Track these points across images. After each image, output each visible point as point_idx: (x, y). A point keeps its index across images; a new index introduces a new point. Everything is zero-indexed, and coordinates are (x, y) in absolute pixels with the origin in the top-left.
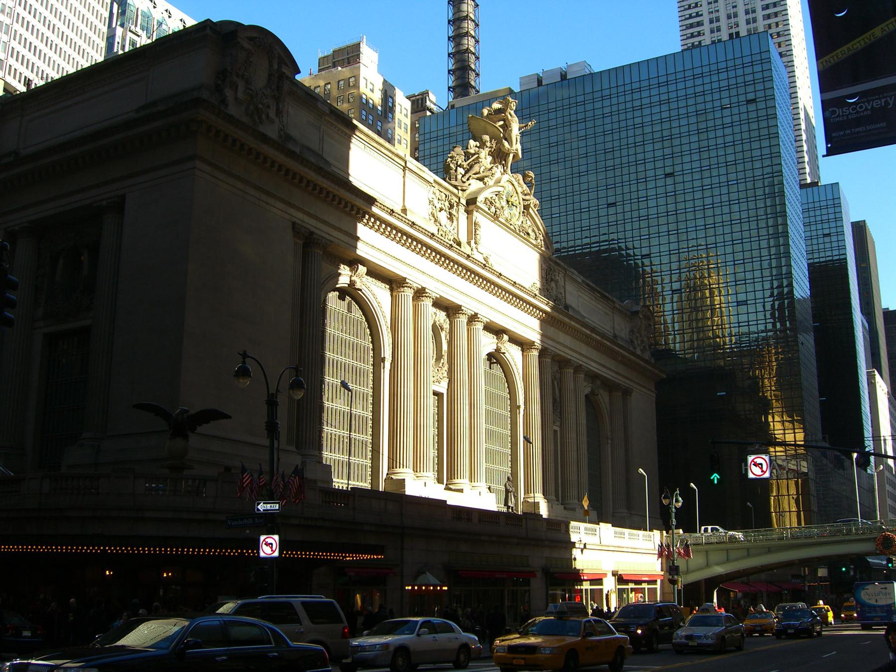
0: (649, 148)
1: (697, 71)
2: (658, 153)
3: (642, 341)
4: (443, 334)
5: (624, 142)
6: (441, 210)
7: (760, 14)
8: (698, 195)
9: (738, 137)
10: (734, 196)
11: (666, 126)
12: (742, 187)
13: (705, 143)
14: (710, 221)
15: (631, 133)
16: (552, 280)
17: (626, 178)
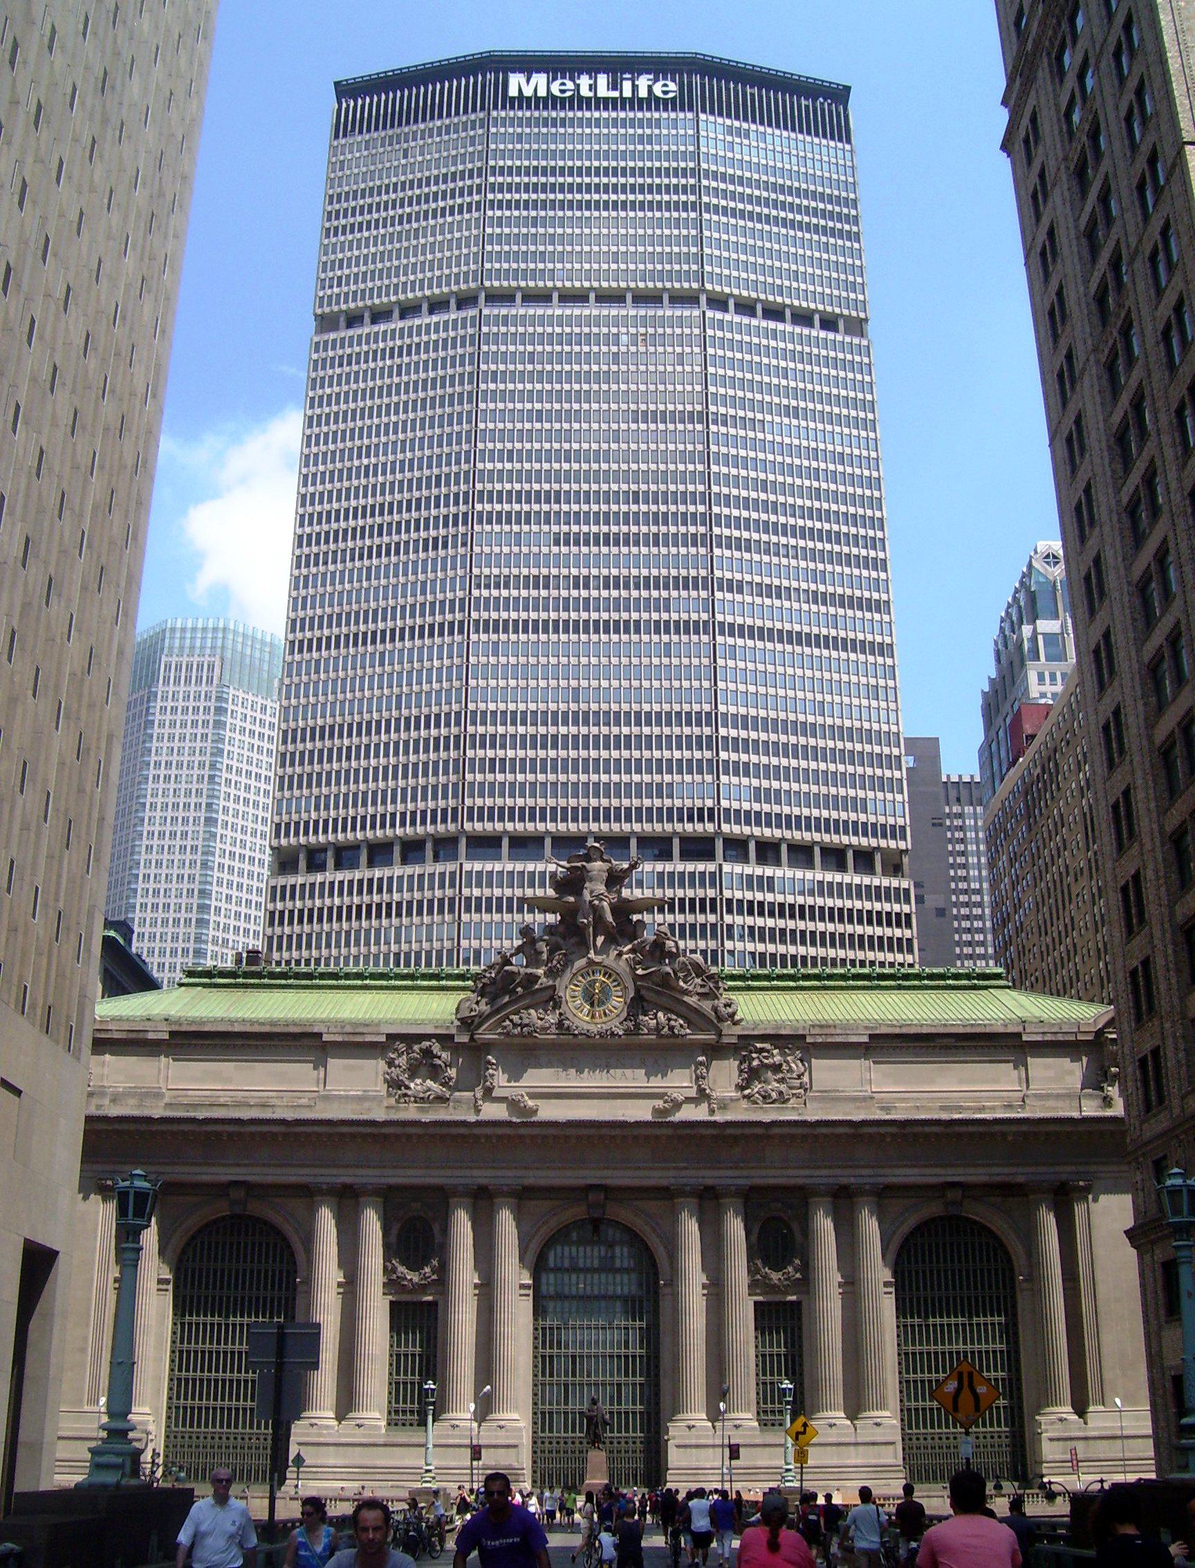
4: (436, 1229)
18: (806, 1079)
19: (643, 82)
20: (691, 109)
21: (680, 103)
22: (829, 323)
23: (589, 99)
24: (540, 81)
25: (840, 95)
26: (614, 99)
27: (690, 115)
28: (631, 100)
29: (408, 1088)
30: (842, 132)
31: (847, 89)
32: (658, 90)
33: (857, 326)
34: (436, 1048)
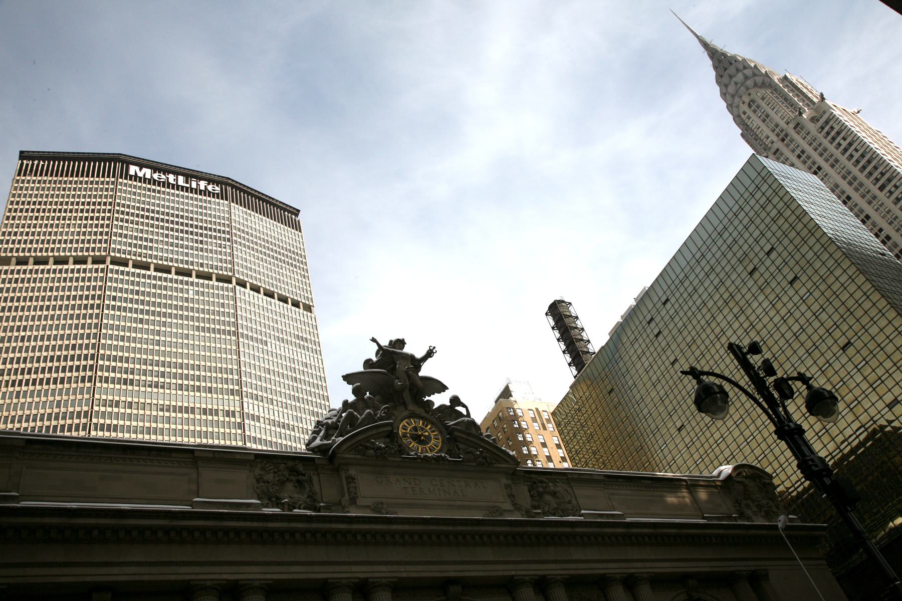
0: (720, 318)
1: (719, 229)
2: (730, 317)
3: (760, 507)
5: (698, 327)
6: (282, 483)
7: (855, 171)
8: (784, 329)
9: (785, 254)
10: (815, 307)
11: (722, 290)
12: (817, 294)
13: (761, 281)
14: (809, 344)
15: (699, 316)
16: (540, 495)
17: (717, 357)
18: (574, 502)
19: (203, 184)
20: (227, 200)
21: (222, 196)
22: (296, 304)
23: (173, 185)
24: (147, 172)
25: (296, 212)
26: (187, 188)
27: (226, 202)
28: (196, 190)
29: (278, 498)
30: (297, 227)
31: (299, 211)
32: (210, 188)
33: (308, 308)
34: (301, 468)
